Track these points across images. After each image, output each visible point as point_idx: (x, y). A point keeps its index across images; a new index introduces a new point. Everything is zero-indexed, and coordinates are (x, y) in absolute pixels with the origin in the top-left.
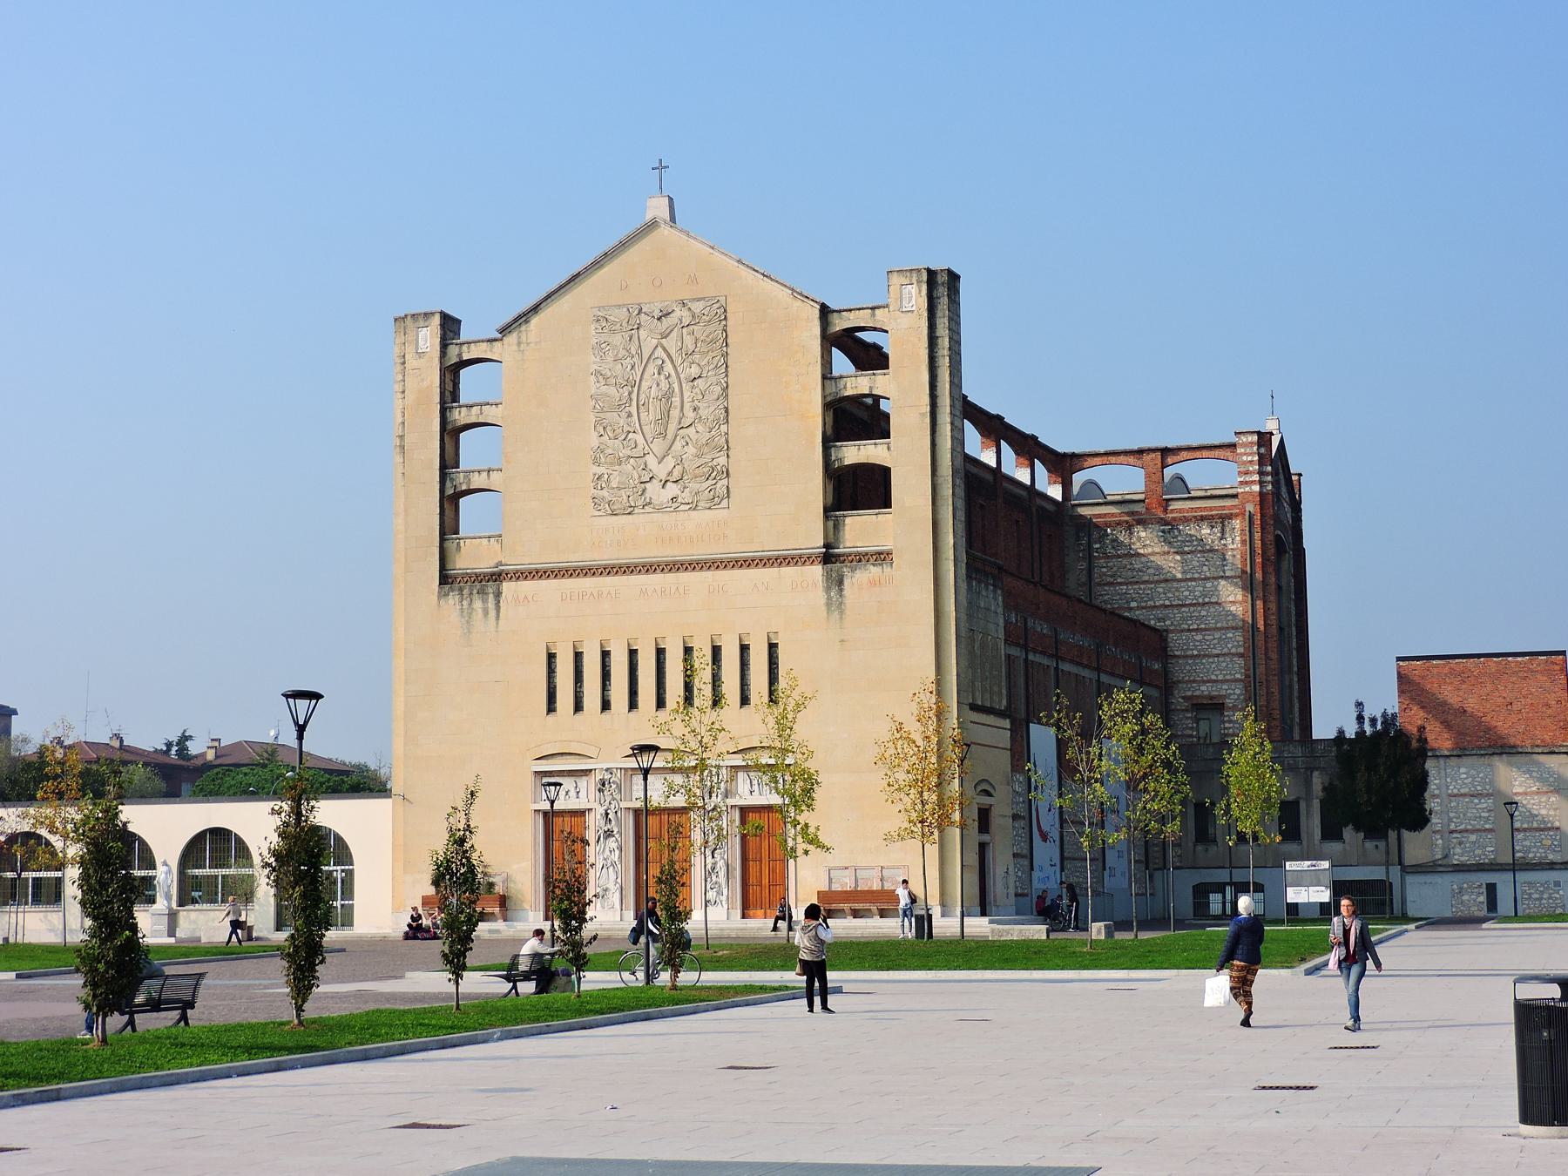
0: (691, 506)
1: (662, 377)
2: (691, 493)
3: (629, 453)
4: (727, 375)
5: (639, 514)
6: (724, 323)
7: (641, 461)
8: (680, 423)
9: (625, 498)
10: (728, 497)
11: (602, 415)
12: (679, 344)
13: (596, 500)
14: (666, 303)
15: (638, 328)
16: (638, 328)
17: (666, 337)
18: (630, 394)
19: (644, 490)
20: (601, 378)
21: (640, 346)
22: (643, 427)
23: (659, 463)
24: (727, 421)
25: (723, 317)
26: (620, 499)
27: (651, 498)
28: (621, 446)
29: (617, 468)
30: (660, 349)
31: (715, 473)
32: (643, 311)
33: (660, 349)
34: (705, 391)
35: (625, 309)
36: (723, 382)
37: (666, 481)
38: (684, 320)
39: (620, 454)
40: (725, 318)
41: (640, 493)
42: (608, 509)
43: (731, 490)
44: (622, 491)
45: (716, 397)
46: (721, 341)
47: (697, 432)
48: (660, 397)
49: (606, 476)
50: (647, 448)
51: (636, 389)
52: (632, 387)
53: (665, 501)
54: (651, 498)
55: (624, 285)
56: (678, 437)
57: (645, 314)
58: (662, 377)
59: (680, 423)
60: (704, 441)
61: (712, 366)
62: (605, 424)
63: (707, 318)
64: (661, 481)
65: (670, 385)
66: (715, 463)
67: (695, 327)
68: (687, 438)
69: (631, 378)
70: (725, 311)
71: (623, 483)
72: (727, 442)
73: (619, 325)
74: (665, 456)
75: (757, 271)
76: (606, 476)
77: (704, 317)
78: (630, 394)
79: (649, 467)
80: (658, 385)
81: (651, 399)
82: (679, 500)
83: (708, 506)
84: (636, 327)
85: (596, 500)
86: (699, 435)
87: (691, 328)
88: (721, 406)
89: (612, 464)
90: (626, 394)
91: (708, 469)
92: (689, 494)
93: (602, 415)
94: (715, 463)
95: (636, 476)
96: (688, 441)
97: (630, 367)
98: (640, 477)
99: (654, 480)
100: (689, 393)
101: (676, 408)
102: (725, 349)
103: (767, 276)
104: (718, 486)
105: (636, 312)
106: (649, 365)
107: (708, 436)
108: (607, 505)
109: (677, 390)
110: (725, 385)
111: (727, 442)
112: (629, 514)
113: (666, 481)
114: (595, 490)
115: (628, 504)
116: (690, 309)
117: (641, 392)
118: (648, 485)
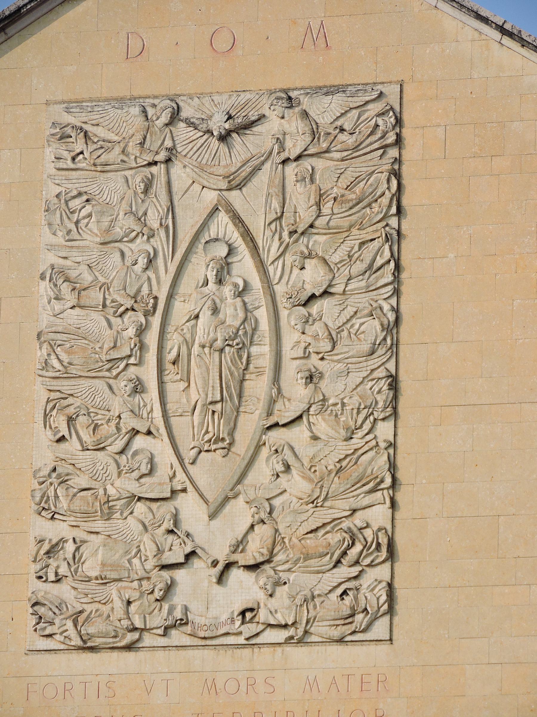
0: (291, 632)
1: (227, 290)
2: (293, 598)
3: (133, 487)
4: (397, 292)
5: (153, 647)
6: (393, 153)
7: (166, 509)
8: (269, 414)
9: (118, 605)
10: (391, 611)
11: (66, 386)
12: (276, 204)
13: (42, 610)
14: (244, 97)
15: (168, 161)
16: (168, 161)
17: (239, 187)
18: (141, 331)
19: (169, 588)
20: (65, 288)
21: (172, 208)
22: (174, 421)
23: (212, 516)
24: (395, 413)
25: (391, 138)
26: (106, 609)
27: (186, 609)
28: (113, 468)
29: (99, 525)
30: (223, 217)
31: (358, 547)
32: (184, 114)
33: (223, 217)
34: (340, 329)
35: (136, 110)
36: (386, 307)
37: (228, 566)
38: (289, 144)
39: (111, 491)
40: (399, 142)
41: (158, 594)
42: (72, 632)
43: (400, 593)
44: (113, 590)
45: (366, 347)
46: (385, 201)
47: (315, 438)
48: (219, 344)
49: (70, 547)
50: (181, 476)
51: (156, 321)
52: (146, 314)
53: (224, 617)
54: (186, 609)
55: (135, 45)
56: (265, 452)
57: (190, 123)
58: (227, 290)
59: (269, 414)
60: (331, 463)
61: (359, 267)
62: (71, 410)
63: (351, 141)
64: (215, 564)
65: (246, 310)
66: (358, 520)
67: (319, 164)
68: (287, 451)
69: (145, 290)
70: (399, 122)
71: (115, 567)
72: (393, 467)
73: (117, 149)
74: (227, 499)
75: (485, 20)
76: (70, 547)
77: (342, 137)
78: (141, 331)
79: (186, 525)
80: (215, 311)
81: (196, 349)
82: (263, 615)
83: (336, 633)
84: (162, 156)
85: (42, 610)
86: (320, 445)
87: (307, 164)
88: (381, 373)
89: (87, 515)
90: (131, 332)
91: (338, 537)
92: (287, 602)
93: (66, 386)
94: (358, 520)
95: (149, 549)
96: (291, 460)
97: (142, 262)
98: (160, 551)
99: (196, 563)
100: (296, 336)
101: (260, 373)
102: (394, 222)
103: (510, 35)
104: (366, 581)
105: (165, 118)
106: (194, 259)
107: (344, 449)
108: (69, 624)
109: (264, 325)
110: (391, 316)
111: (393, 467)
112: (129, 647)
113: (228, 566)
114: (40, 584)
115: (125, 623)
116: (305, 114)
117: (170, 329)
118: (180, 575)
